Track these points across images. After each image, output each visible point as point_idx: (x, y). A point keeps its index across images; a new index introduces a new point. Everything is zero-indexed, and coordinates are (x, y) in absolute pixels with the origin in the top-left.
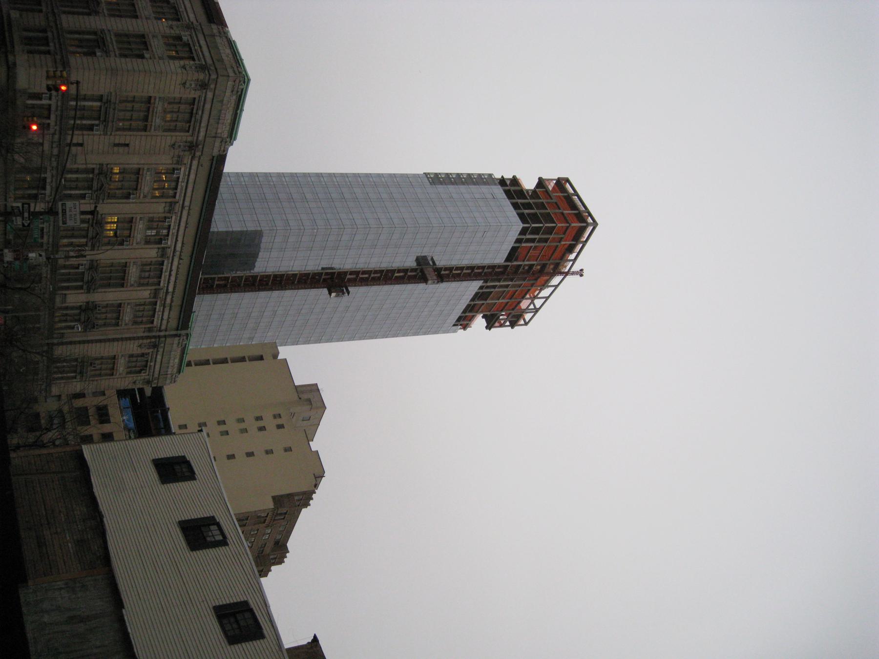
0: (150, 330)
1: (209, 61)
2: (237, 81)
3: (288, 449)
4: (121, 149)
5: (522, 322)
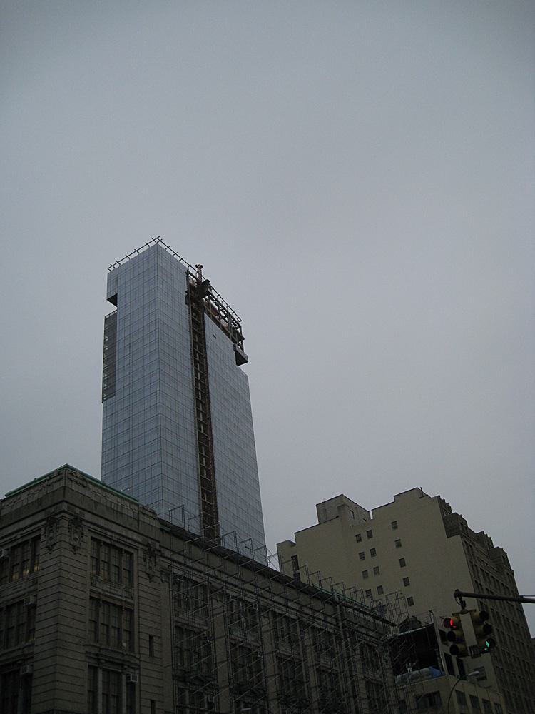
0: (338, 638)
1: (41, 516)
2: (71, 477)
3: (395, 525)
4: (156, 647)
5: (238, 330)
